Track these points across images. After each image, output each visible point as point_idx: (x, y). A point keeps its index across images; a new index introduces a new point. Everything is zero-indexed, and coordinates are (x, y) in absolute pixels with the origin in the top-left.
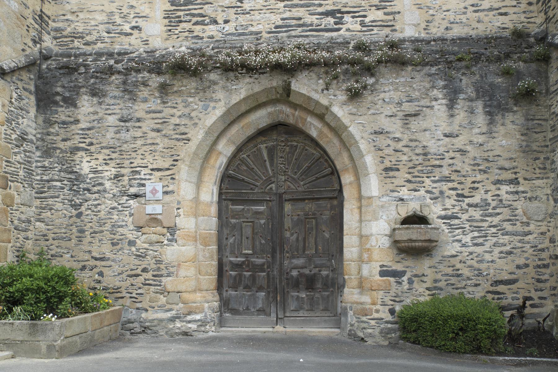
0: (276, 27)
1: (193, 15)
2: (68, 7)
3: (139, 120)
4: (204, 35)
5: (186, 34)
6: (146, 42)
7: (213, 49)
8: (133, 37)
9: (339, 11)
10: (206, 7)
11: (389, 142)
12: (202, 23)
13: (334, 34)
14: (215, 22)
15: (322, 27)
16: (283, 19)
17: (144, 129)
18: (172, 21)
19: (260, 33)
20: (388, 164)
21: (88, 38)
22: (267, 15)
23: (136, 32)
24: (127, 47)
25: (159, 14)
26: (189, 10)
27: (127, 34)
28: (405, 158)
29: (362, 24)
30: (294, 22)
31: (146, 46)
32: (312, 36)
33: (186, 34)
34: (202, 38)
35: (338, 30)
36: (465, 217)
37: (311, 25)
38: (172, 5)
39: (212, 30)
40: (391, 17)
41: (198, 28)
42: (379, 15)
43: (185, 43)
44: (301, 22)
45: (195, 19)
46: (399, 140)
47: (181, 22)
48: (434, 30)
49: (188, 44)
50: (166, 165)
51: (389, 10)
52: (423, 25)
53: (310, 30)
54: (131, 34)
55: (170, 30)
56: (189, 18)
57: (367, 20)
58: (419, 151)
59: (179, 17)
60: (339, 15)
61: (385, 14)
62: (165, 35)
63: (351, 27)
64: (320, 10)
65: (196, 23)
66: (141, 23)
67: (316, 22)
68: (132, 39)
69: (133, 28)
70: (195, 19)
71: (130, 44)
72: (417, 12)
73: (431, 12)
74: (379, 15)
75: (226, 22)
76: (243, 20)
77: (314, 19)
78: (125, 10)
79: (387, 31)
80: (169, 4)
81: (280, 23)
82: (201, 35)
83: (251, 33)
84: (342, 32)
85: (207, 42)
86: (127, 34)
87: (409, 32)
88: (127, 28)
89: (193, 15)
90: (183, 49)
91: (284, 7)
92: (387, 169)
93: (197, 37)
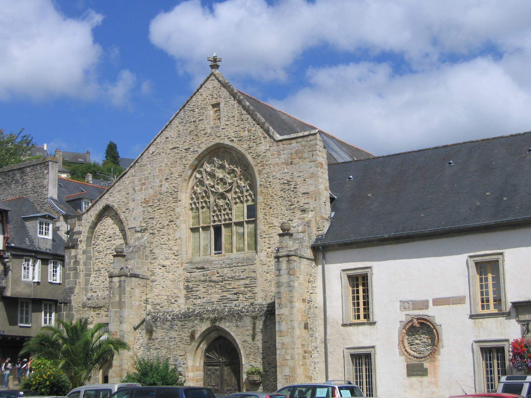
2: (155, 294)
3: (175, 338)
9: (238, 293)
11: (247, 345)
14: (200, 298)
17: (177, 341)
18: (187, 298)
20: (247, 352)
21: (162, 305)
28: (252, 350)
29: (245, 298)
30: (224, 298)
35: (238, 300)
36: (271, 371)
41: (195, 300)
42: (250, 294)
45: (194, 297)
46: (251, 344)
50: (183, 354)
51: (253, 292)
52: (264, 298)
57: (247, 296)
58: (256, 348)
64: (232, 293)
65: (195, 299)
66: (177, 299)
67: (231, 297)
68: (175, 305)
69: (175, 301)
70: (194, 297)
74: (250, 294)
75: (204, 298)
77: (231, 296)
78: (172, 295)
81: (220, 298)
83: (211, 302)
88: (173, 301)
92: (247, 355)
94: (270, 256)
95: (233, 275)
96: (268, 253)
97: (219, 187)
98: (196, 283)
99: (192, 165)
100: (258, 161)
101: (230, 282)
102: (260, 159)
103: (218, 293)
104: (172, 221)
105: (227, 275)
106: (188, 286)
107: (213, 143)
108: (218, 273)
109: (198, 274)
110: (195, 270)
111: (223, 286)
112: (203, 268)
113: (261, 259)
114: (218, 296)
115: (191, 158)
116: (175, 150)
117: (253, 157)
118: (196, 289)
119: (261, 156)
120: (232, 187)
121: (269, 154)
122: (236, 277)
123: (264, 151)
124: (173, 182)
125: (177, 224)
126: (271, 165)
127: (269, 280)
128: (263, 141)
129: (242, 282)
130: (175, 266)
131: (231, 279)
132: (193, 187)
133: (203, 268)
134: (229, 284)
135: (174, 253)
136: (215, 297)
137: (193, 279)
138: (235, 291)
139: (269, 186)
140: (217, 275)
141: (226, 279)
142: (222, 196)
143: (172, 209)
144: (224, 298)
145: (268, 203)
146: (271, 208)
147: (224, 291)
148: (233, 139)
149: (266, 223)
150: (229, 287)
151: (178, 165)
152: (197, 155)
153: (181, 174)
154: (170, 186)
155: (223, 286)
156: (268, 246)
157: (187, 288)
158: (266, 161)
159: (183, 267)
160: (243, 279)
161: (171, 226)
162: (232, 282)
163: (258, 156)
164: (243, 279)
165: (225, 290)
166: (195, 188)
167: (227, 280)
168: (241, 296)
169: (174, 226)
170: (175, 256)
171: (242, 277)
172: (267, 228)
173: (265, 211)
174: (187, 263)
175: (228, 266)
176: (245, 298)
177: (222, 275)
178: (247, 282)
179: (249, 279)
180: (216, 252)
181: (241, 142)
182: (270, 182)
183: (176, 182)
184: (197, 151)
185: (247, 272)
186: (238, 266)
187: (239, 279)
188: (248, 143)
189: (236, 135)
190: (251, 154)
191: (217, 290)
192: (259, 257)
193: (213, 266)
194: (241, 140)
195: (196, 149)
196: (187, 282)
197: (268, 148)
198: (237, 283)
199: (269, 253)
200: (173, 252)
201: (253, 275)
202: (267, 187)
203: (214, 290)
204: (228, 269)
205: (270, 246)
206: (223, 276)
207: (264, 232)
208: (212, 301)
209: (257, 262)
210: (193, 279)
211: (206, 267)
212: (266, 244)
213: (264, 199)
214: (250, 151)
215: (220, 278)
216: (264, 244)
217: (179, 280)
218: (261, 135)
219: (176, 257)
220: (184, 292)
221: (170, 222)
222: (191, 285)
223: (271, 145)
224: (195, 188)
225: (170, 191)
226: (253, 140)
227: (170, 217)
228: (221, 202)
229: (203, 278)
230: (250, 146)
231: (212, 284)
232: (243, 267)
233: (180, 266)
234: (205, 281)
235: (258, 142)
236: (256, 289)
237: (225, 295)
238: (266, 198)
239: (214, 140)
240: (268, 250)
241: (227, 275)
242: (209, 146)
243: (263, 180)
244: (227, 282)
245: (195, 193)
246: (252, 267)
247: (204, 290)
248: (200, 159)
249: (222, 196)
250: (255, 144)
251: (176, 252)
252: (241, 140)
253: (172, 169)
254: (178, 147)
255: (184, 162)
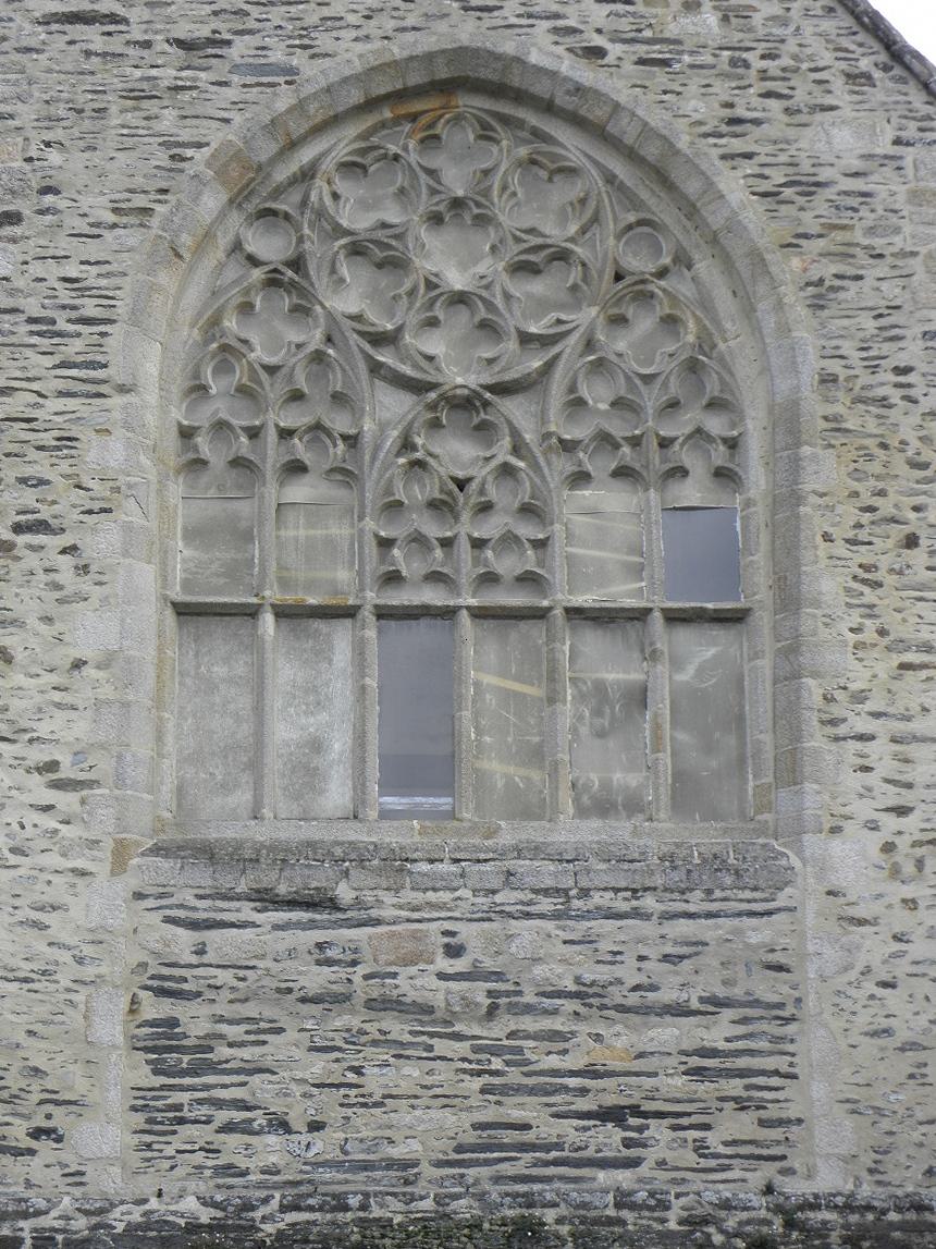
0: (459, 1149)
1: (219, 1104)
4: (251, 1164)
5: (199, 1158)
6: (76, 1177)
7: (284, 1209)
8: (37, 1162)
9: (636, 1111)
10: (256, 1079)
12: (245, 1128)
13: (624, 1178)
14: (282, 1125)
15: (590, 1153)
16: (477, 1126)
18: (157, 1119)
19: (415, 1164)
22: (433, 1113)
23: (44, 1146)
24: (20, 1191)
25: (115, 1098)
26: (207, 1087)
27: (18, 1152)
29: (700, 1148)
30: (509, 1136)
31: (77, 1192)
32: (561, 1178)
33: (199, 1158)
34: (244, 1173)
35: (634, 1163)
37: (558, 1146)
38: (156, 1072)
39: (271, 1149)
40: (776, 1134)
41: (234, 1140)
42: (743, 1125)
43: (192, 1185)
44: (529, 1136)
45: (223, 1116)
47: (182, 1121)
48: (894, 1176)
49: (202, 1188)
51: (773, 1112)
52: (867, 1159)
53: (556, 1163)
54: (31, 1152)
55: (149, 1146)
56: (204, 1110)
57: (713, 1140)
59: (178, 1107)
60: (632, 1121)
61: (762, 1123)
62: (135, 1160)
63: (669, 1156)
64: (583, 1104)
67: (573, 1137)
68: (35, 1167)
69: (37, 1134)
70: (223, 1116)
71: (28, 1184)
72: (849, 1123)
73: (885, 1124)
74: (743, 1125)
75: (316, 1126)
76: (366, 1124)
79: (768, 1171)
80: (147, 1069)
81: (471, 1137)
82: (242, 1163)
83: (391, 1164)
84: (644, 1170)
85: (260, 1185)
86: (18, 1152)
87: (829, 1180)
89: (219, 1104)
90: (190, 1204)
91: (483, 1091)
93: (228, 1169)
94: (909, 869)
95: (602, 973)
96: (888, 848)
97: (434, 344)
98: (250, 1010)
99: (237, 156)
100: (807, 217)
101: (557, 1024)
102: (820, 203)
103: (448, 1101)
104: (42, 527)
105: (539, 971)
106: (173, 1023)
107: (426, 43)
108: (454, 951)
109: (271, 942)
110: (247, 911)
111: (495, 1051)
112: (319, 902)
113: (835, 881)
114: (456, 1124)
115: (229, 115)
116: (93, 36)
117: (765, 186)
118: (246, 1053)
119: (830, 193)
120: (549, 366)
121: (888, 188)
122: (616, 995)
123: (857, 164)
124: (64, 245)
125: (88, 554)
126: (916, 264)
127: (903, 1035)
128: (840, 94)
129: (667, 1034)
130: (54, 860)
131: (571, 1006)
132: (215, 321)
133: (319, 902)
134: (554, 1036)
135: (52, 766)
136: (423, 1133)
137: (225, 977)
138: (609, 1093)
139: (895, 396)
140: (444, 964)
141: (529, 998)
142: (468, 409)
143: (47, 439)
144: (509, 1136)
145: (886, 507)
146: (911, 542)
147: (506, 1090)
148: (599, 41)
149: (869, 635)
150: (554, 1061)
151: (111, 139)
152: (284, 100)
153: (140, 201)
154: (36, 269)
155: (495, 1051)
156: (893, 796)
157: (160, 1043)
158: (871, 231)
159: (132, 882)
160: (680, 1011)
161: (32, 561)
162: (583, 1028)
163: (810, 187)
164: (680, 1011)
165: (514, 1076)
166: (231, 323)
167: (528, 1009)
168: (658, 1131)
169: (66, 561)
170: (58, 785)
171: (667, 995)
172: (885, 666)
173: (864, 555)
174: (157, 850)
175: (546, 905)
176: (700, 1148)
177: (489, 964)
178: (718, 1032)
179: (728, 1014)
180: (393, 802)
181: (660, 77)
182: (899, 371)
183: (93, 250)
184: (291, 71)
185: (710, 960)
186: (636, 914)
187: (644, 1010)
188: (722, 90)
189: (624, 25)
190: (749, 168)
191: (444, 1074)
192: (823, 869)
193: (418, 897)
194: (665, 63)
195: (277, 56)
196: (162, 992)
197: (884, 146)
198: (621, 1040)
199: (903, 844)
200: (38, 755)
201: (767, 988)
202: (883, 402)
203: (413, 1071)
204: (550, 925)
205: (907, 798)
206: (498, 976)
207: (860, 697)
208: (395, 1152)
209: (805, 893)
210: (225, 977)
211: (344, 892)
212: (872, 779)
213: (857, 474)
214: (737, 145)
215: (479, 992)
216: (855, 781)
217: (89, 972)
218: (827, 58)
219: (66, 801)
220: (129, 1072)
221: (18, 529)
222: (195, 1020)
223: (911, 131)
224: (231, 323)
225: (37, 312)
226: (764, 75)
227: (29, 497)
228: (456, 452)
229: (315, 979)
230: (740, 112)
231: (398, 1028)
232: (683, 927)
233: (102, 869)
234: (333, 1000)
235: (800, 97)
236: (791, 1090)
237: (516, 1115)
238: (875, 467)
239: (442, 27)
240: (890, 822)
241: (539, 971)
242: (397, 51)
243: (848, 348)
244: (529, 1024)
245: (228, 354)
246: (759, 933)
247: (318, 1067)
248: (298, 128)
249: (468, 409)
250: (773, 103)
251: (65, 760)
252: (665, 63)
253: (54, 157)
254: (113, 18)
255: (168, 121)
